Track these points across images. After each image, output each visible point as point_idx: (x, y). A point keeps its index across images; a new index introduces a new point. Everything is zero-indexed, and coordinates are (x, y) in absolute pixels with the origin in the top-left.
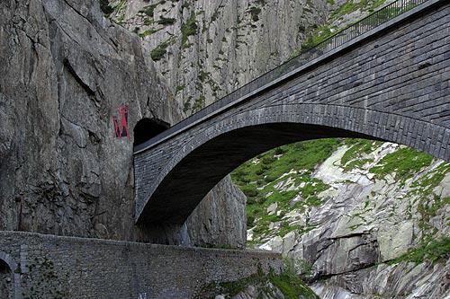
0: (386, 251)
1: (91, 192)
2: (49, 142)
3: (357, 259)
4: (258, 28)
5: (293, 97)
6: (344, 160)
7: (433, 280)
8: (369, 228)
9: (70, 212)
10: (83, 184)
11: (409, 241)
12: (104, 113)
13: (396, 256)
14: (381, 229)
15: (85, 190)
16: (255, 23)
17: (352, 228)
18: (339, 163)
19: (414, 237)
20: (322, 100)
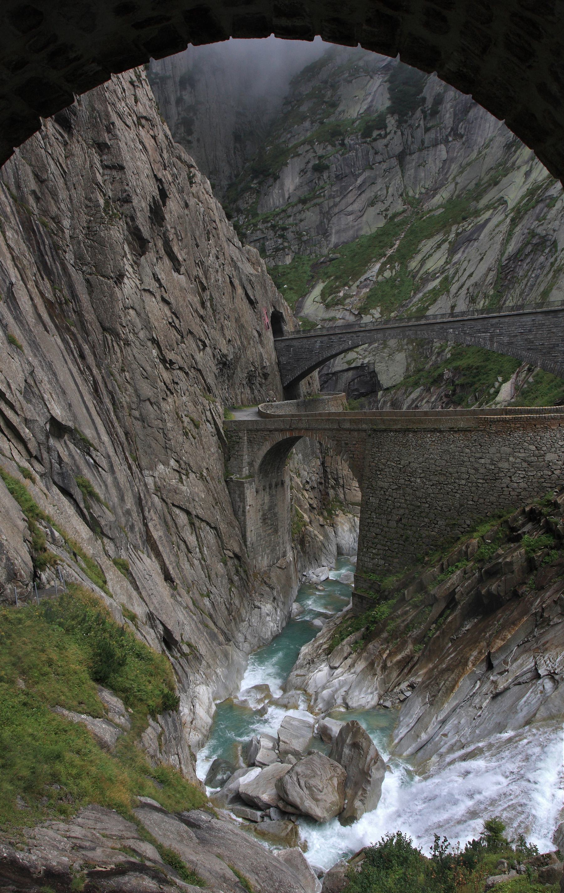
0: (385, 380)
1: (268, 371)
2: (250, 344)
3: (357, 390)
4: (195, 144)
5: (451, 330)
6: (323, 294)
7: (433, 400)
8: (366, 361)
9: (258, 386)
10: (265, 367)
11: (403, 370)
12: (260, 318)
13: (394, 383)
14: (377, 361)
15: (266, 371)
16: (190, 138)
17: (349, 363)
18: (319, 299)
19: (408, 365)
20: (470, 335)
